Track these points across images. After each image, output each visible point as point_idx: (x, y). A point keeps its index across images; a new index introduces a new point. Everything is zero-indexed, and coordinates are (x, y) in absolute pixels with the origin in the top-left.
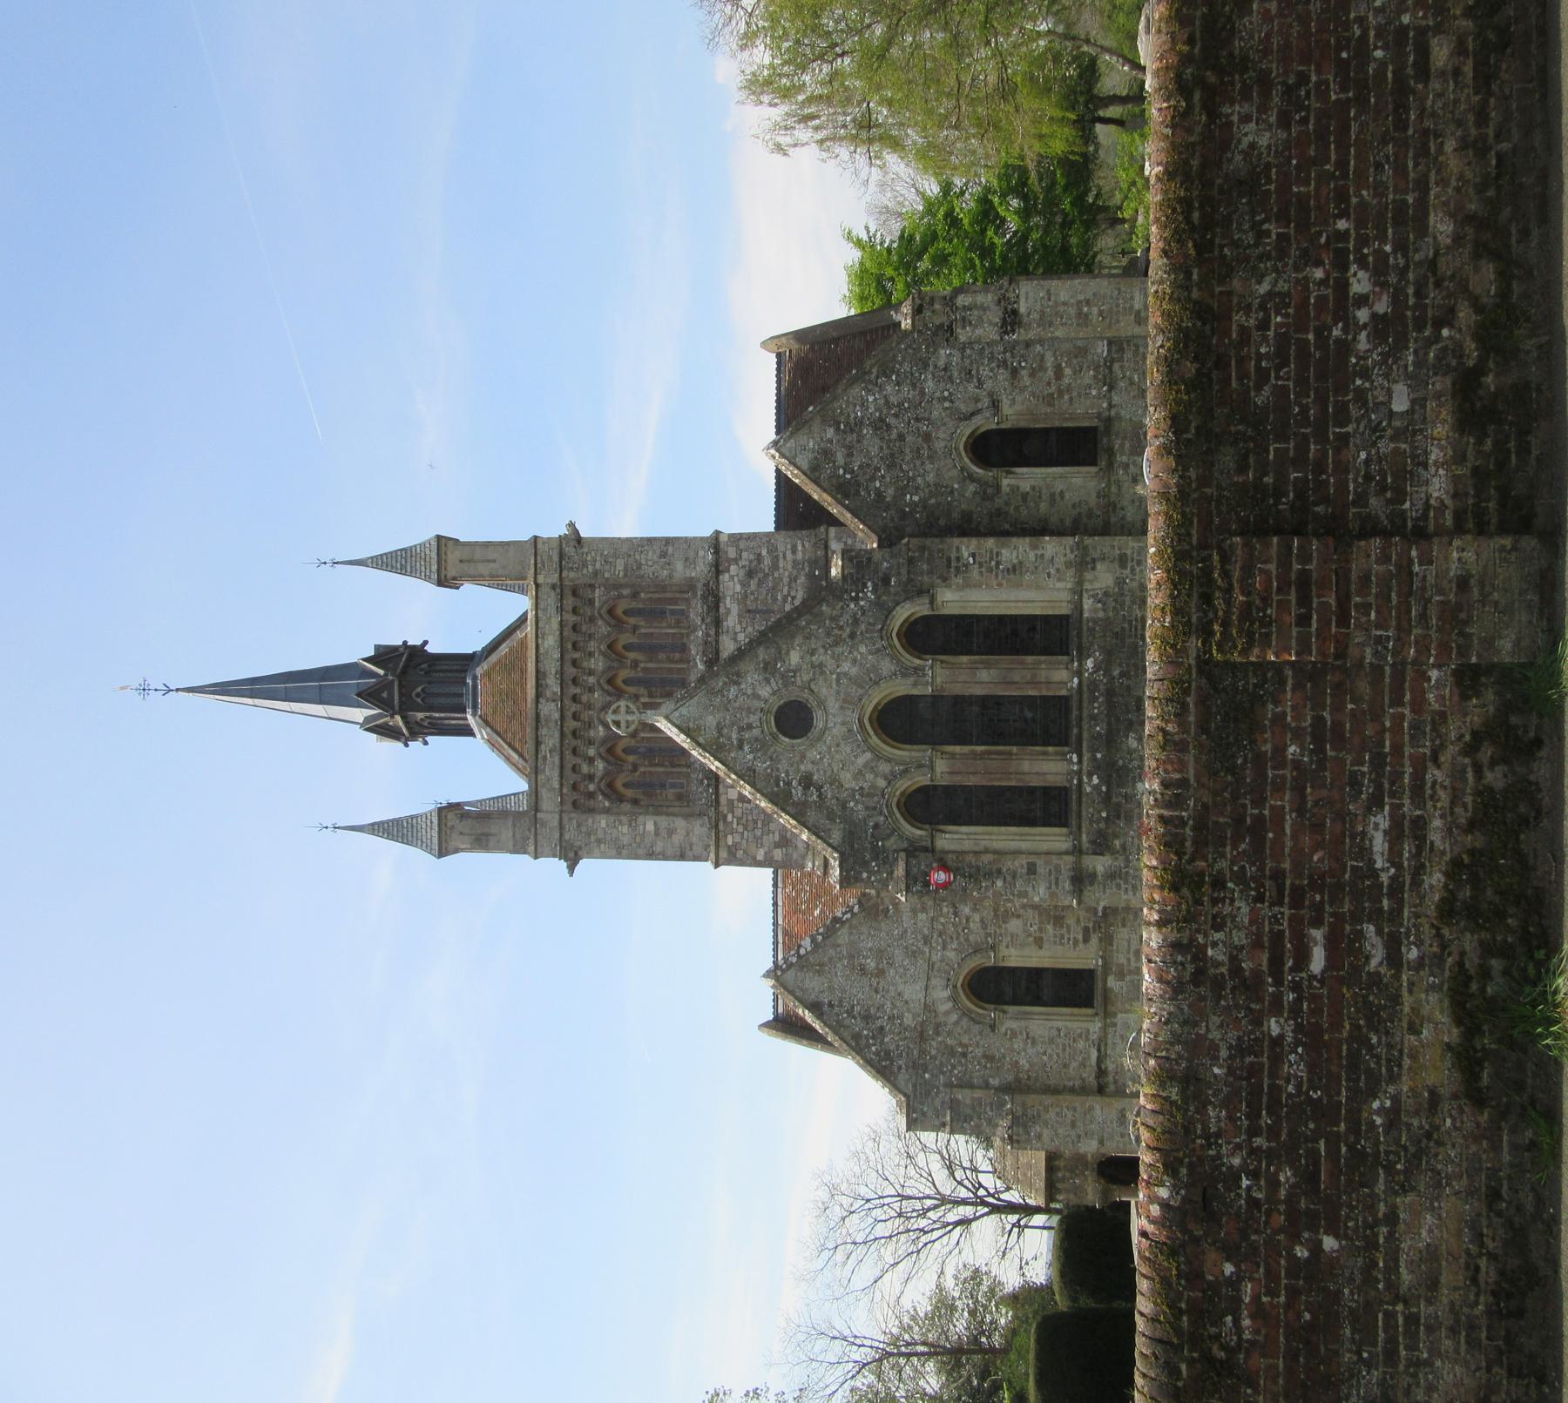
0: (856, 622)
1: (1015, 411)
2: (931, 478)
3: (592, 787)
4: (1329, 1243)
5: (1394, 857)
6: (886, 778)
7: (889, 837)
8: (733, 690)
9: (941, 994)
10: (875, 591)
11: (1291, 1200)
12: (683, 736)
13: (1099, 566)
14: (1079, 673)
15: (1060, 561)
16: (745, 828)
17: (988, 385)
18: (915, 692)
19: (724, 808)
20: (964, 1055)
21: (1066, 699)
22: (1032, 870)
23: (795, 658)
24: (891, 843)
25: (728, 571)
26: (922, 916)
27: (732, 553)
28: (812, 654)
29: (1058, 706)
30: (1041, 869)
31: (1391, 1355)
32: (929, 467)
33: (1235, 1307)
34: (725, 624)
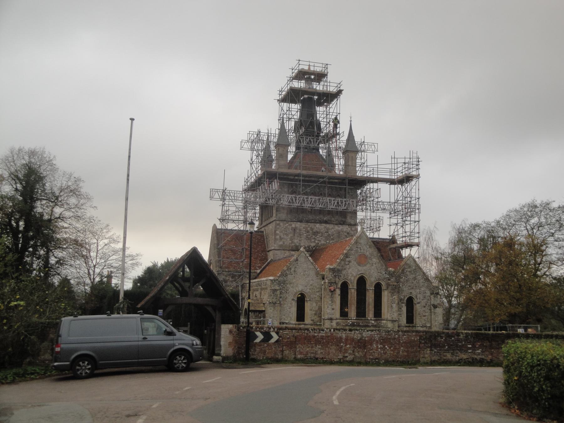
0: (381, 273)
1: (418, 308)
2: (405, 289)
3: (294, 187)
4: (447, 347)
5: (477, 353)
6: (350, 279)
7: (338, 279)
8: (368, 247)
9: (300, 288)
10: (387, 277)
11: (450, 344)
12: (359, 235)
13: (392, 324)
14: (371, 320)
15: (393, 316)
16: (285, 229)
17: (423, 301)
18: (367, 285)
19: (290, 223)
20: (287, 293)
21: (365, 317)
22: (333, 309)
23: (374, 260)
24: (337, 279)
25: (349, 228)
26: (316, 284)
27: (353, 229)
28: (375, 264)
29: (364, 316)
30: (333, 311)
31: (438, 352)
32: (407, 288)
33: (441, 339)
34: (336, 226)
